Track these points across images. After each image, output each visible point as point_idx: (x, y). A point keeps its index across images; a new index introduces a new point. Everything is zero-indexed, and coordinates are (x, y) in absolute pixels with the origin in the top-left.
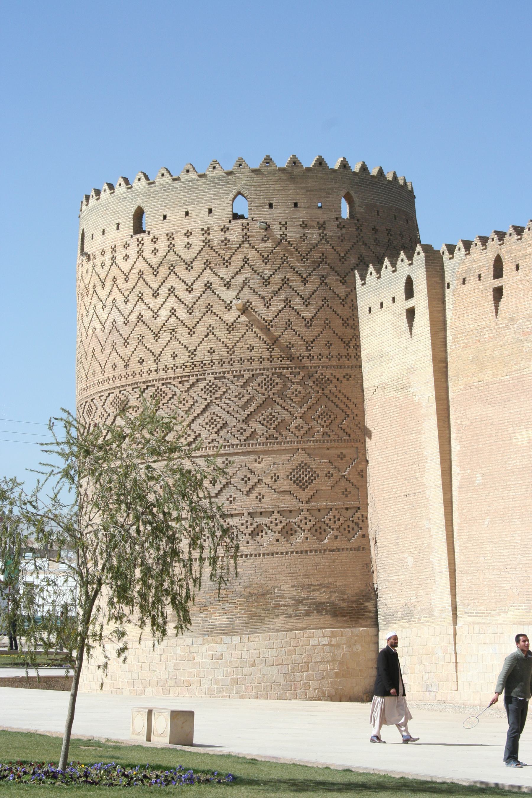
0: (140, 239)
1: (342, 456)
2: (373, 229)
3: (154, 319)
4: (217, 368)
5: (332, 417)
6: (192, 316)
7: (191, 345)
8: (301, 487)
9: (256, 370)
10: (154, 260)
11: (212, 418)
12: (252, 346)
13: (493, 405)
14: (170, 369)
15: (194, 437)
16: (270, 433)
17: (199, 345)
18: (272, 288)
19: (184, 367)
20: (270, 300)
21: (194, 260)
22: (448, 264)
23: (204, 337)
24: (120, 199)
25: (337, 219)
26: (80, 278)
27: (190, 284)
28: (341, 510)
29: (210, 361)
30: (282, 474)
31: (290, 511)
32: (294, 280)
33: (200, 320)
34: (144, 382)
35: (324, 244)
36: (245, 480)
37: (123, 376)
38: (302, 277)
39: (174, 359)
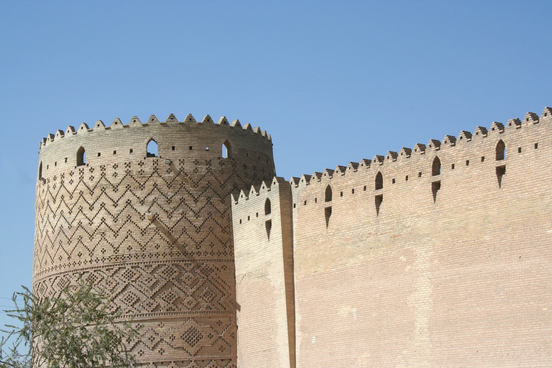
0: (81, 169)
1: (219, 323)
2: (244, 166)
3: (89, 225)
4: (134, 260)
5: (214, 295)
6: (117, 223)
7: (115, 244)
8: (190, 344)
9: (161, 262)
10: (91, 184)
11: (129, 295)
12: (158, 245)
13: (324, 289)
14: (100, 260)
15: (116, 309)
16: (169, 306)
17: (121, 244)
18: (173, 205)
19: (110, 259)
20: (172, 213)
21: (119, 185)
22: (295, 191)
23: (125, 238)
24: (68, 141)
25: (219, 158)
26: (38, 196)
27: (116, 201)
28: (219, 361)
29: (128, 255)
30: (177, 335)
31: (183, 362)
32: (188, 200)
33: (122, 226)
34: (81, 270)
35: (210, 175)
36: (151, 339)
37: (67, 265)
38: (194, 198)
39: (103, 253)
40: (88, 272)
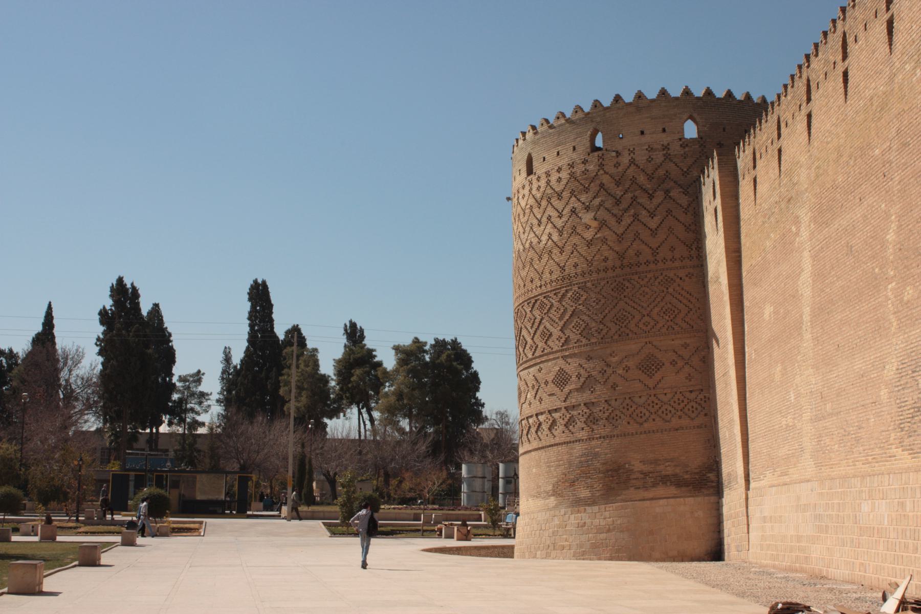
1: (685, 346)
2: (718, 144)
4: (581, 279)
5: (676, 311)
10: (538, 195)
11: (577, 322)
18: (624, 205)
20: (621, 216)
25: (680, 139)
40: (538, 299)
